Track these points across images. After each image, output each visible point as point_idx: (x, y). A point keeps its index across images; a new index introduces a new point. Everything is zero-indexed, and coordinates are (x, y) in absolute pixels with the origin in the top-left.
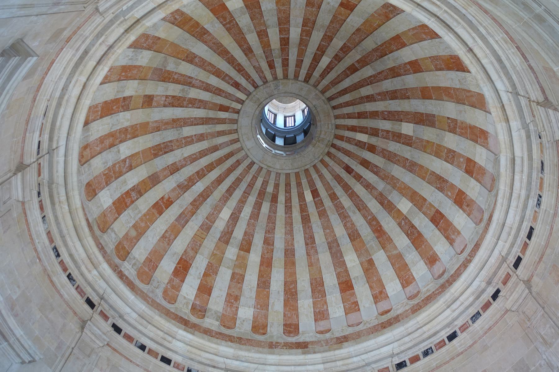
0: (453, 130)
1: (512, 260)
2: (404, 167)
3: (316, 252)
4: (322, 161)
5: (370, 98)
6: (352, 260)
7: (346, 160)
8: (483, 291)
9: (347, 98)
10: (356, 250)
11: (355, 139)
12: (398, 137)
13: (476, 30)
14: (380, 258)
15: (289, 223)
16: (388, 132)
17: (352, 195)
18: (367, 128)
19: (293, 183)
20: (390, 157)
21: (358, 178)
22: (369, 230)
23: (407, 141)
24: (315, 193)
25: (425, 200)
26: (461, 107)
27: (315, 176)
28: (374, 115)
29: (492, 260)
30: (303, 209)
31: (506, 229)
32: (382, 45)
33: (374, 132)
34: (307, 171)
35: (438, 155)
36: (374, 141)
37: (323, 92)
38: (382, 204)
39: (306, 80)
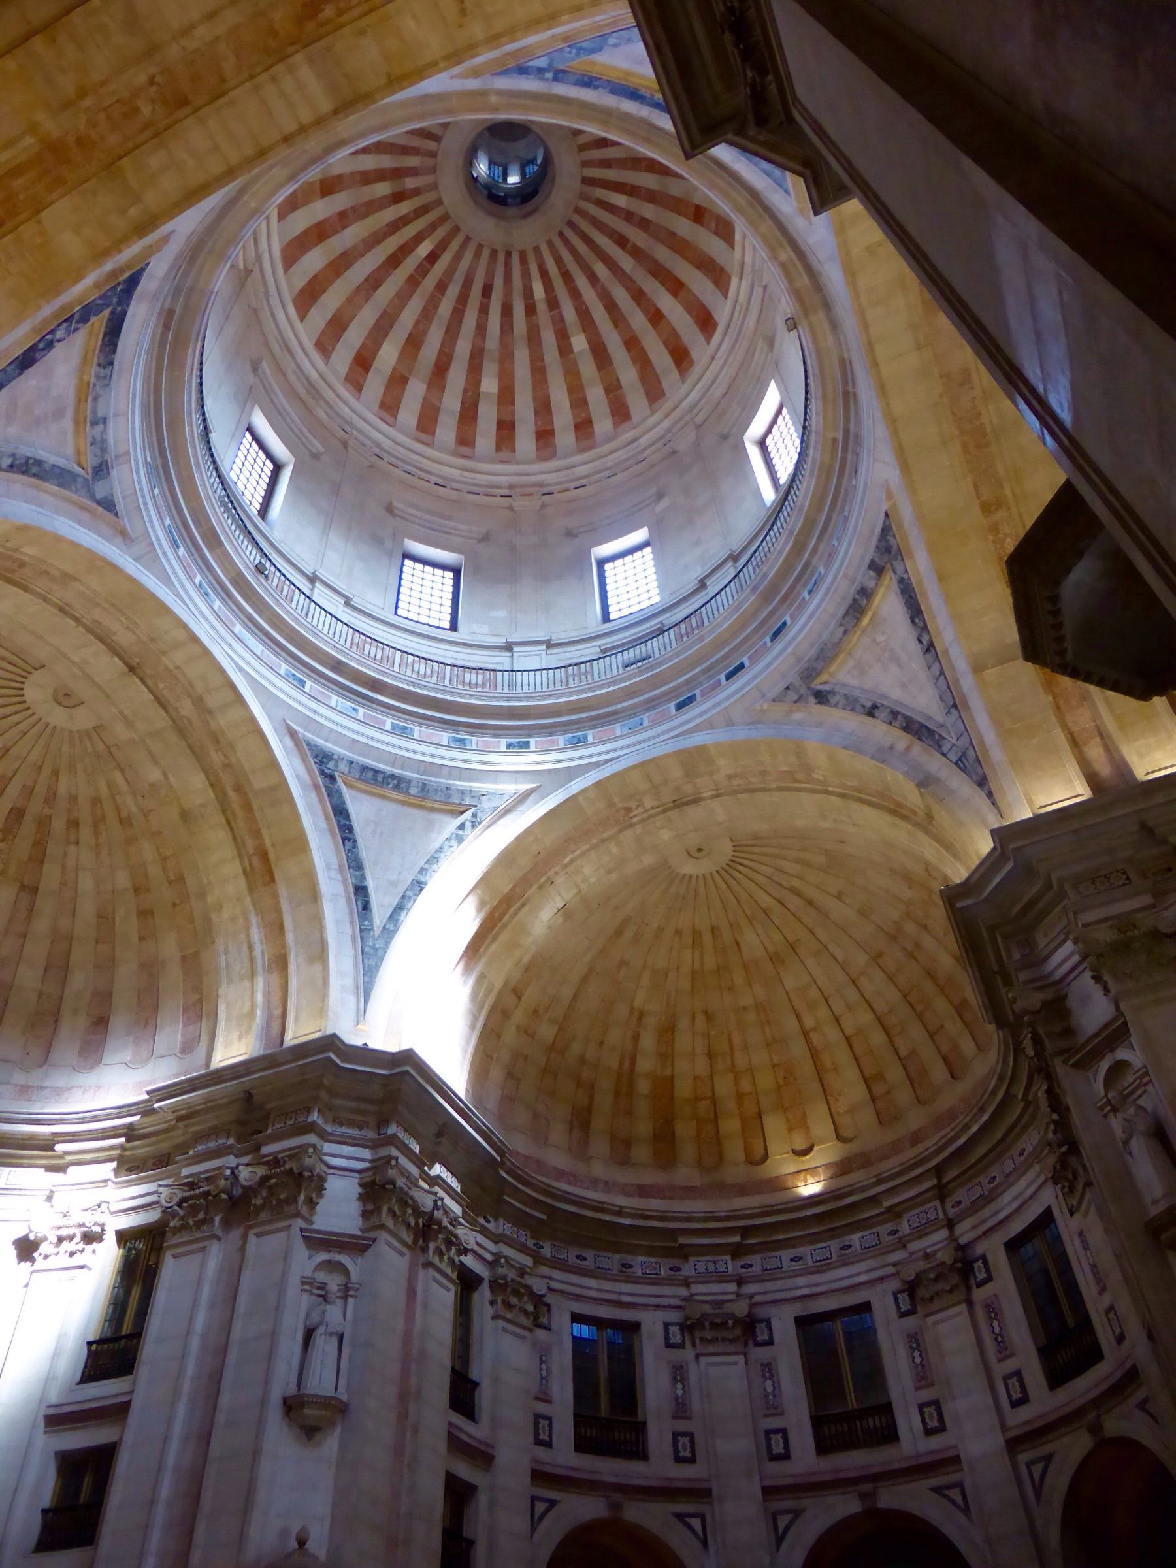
0: (608, 390)
1: (546, 490)
2: (532, 361)
3: (367, 300)
4: (480, 247)
5: (593, 279)
6: (388, 355)
7: (498, 282)
8: (500, 487)
9: (581, 247)
10: (402, 354)
11: (530, 281)
12: (563, 336)
13: (730, 353)
14: (416, 390)
15: (376, 239)
16: (562, 320)
17: (458, 314)
18: (553, 290)
19: (431, 216)
20: (534, 338)
21: (484, 310)
22: (434, 357)
23: (565, 349)
24: (432, 258)
25: (513, 403)
26: (638, 385)
27: (455, 245)
28: (575, 294)
29: (534, 479)
30: (406, 249)
31: (569, 471)
32: (666, 269)
33: (553, 303)
34: (456, 230)
35: (570, 391)
36: (542, 307)
37: (578, 211)
38: (472, 357)
39: (587, 181)
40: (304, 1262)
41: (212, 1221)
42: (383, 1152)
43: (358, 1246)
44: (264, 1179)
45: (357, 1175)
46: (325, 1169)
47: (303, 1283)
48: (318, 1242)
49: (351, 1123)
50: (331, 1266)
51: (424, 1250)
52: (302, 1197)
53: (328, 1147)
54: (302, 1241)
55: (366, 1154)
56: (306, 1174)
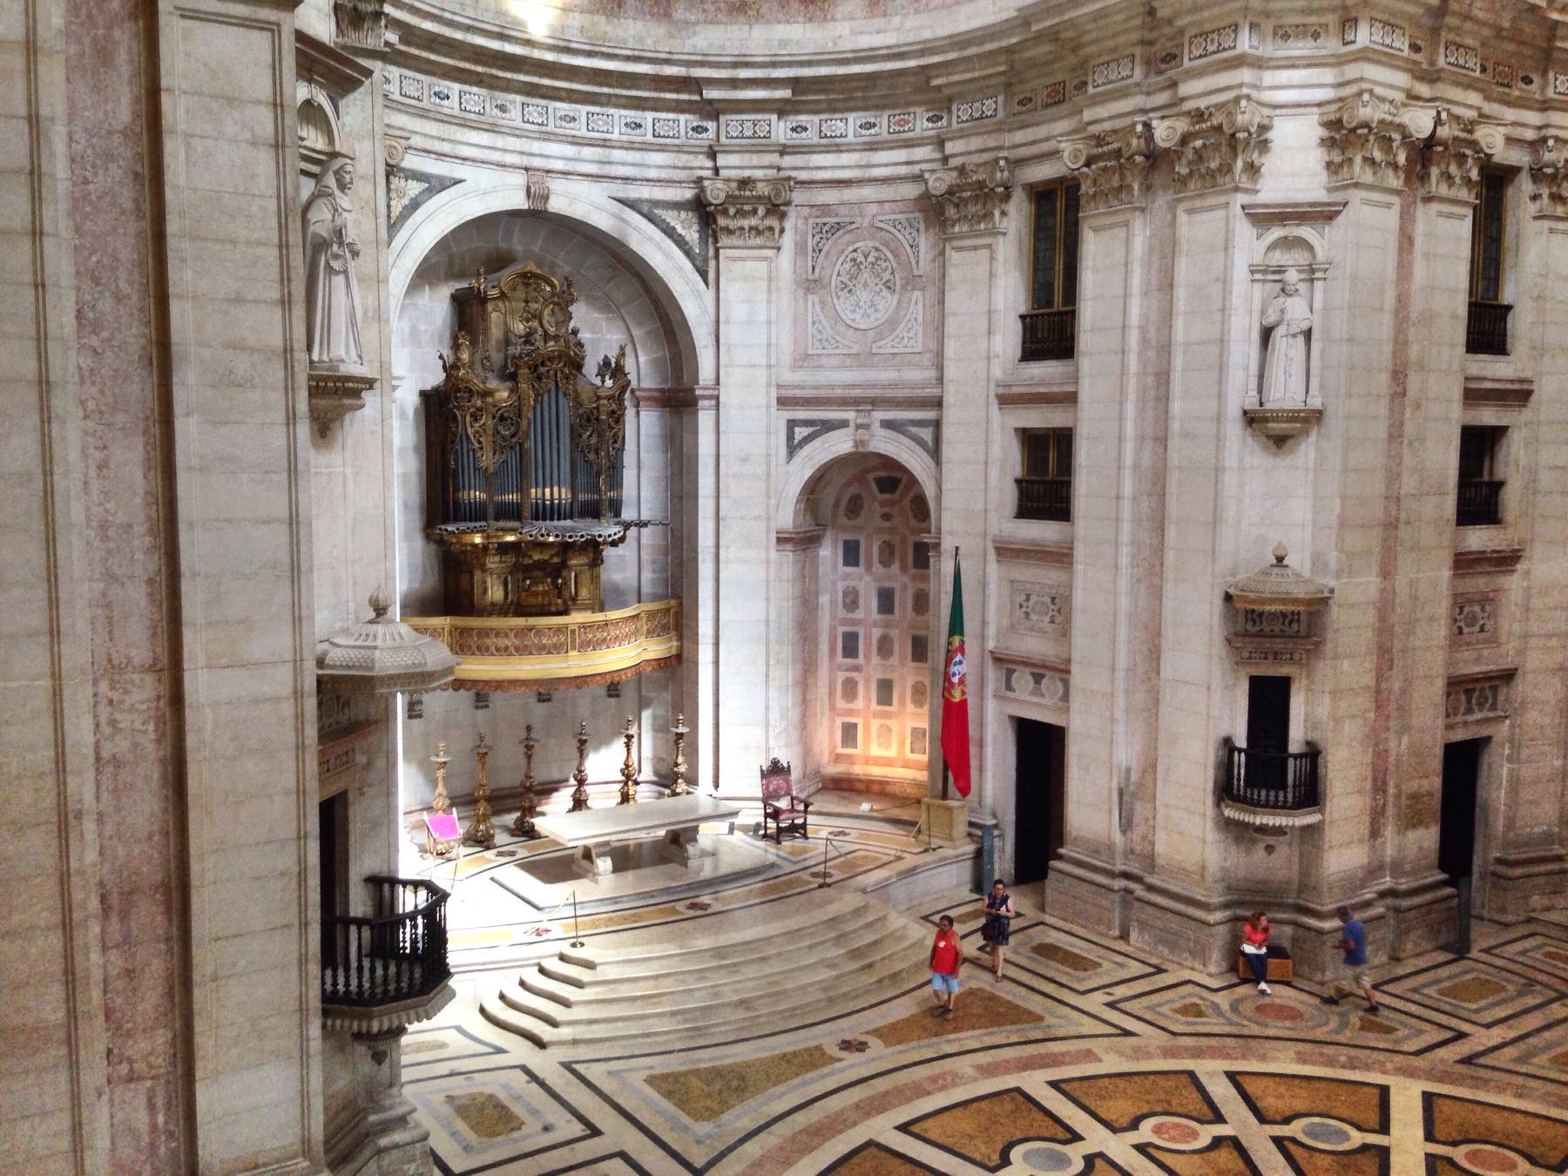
40: (1250, 246)
41: (1130, 187)
42: (1352, 71)
43: (1323, 215)
44: (1185, 140)
45: (1315, 110)
46: (1266, 111)
47: (1252, 272)
48: (1264, 218)
49: (1302, 31)
50: (1285, 243)
51: (1424, 178)
52: (1239, 164)
53: (1269, 77)
54: (1245, 219)
55: (1328, 75)
56: (1241, 135)
